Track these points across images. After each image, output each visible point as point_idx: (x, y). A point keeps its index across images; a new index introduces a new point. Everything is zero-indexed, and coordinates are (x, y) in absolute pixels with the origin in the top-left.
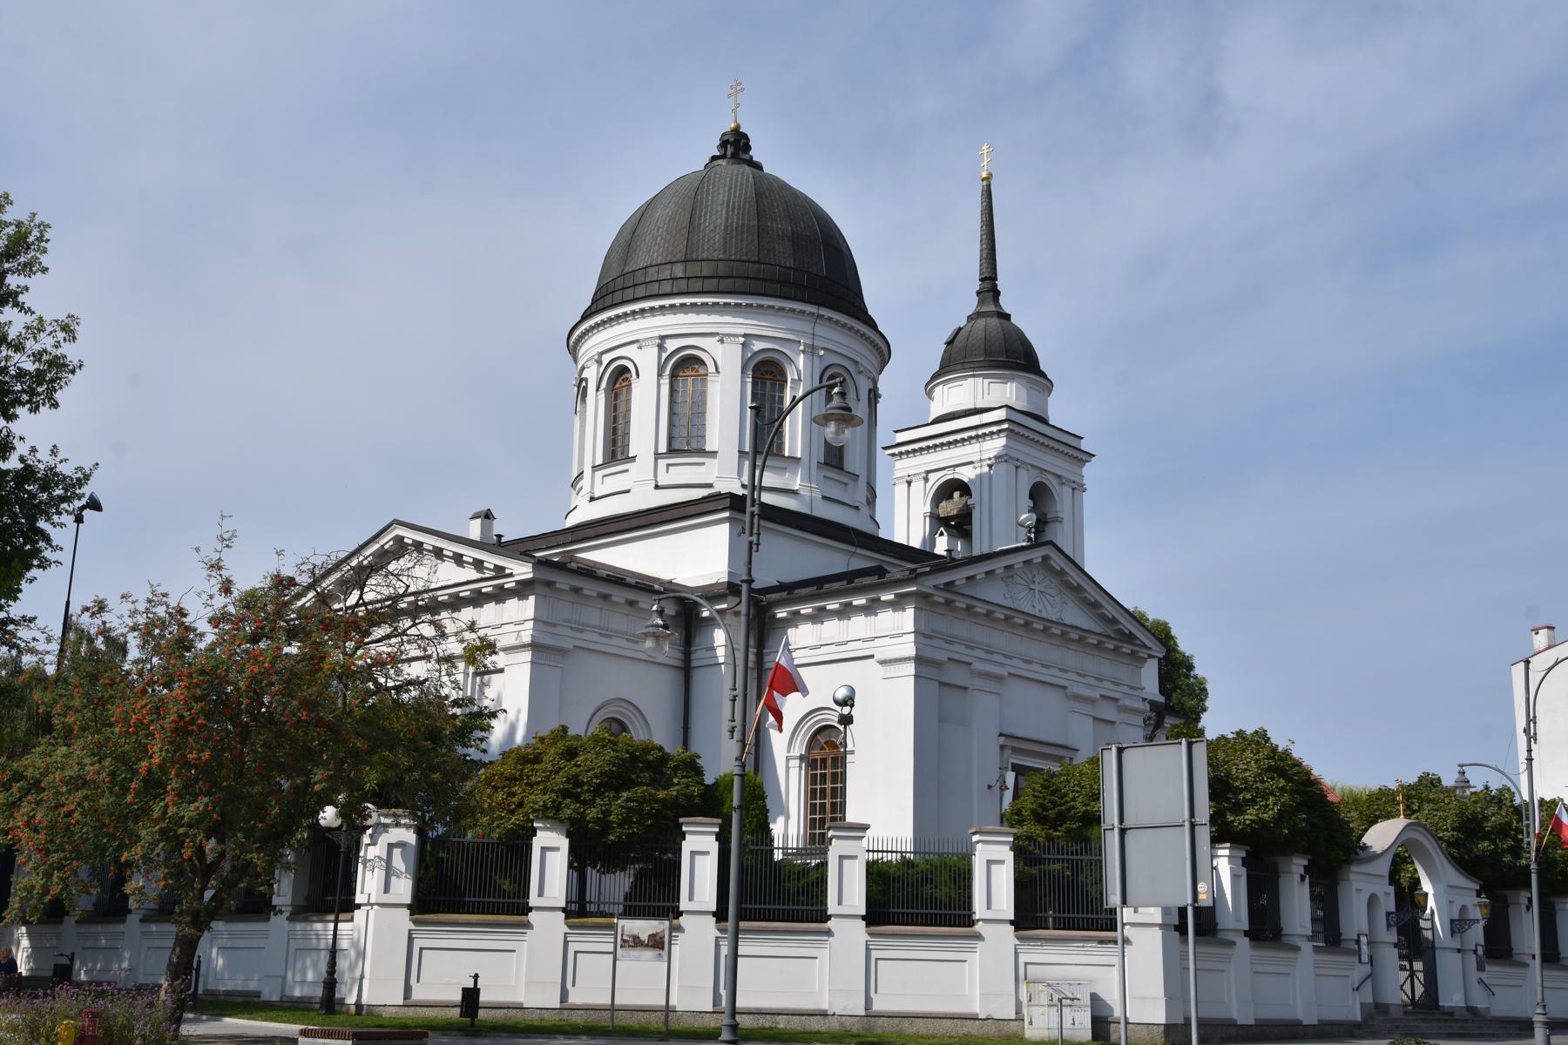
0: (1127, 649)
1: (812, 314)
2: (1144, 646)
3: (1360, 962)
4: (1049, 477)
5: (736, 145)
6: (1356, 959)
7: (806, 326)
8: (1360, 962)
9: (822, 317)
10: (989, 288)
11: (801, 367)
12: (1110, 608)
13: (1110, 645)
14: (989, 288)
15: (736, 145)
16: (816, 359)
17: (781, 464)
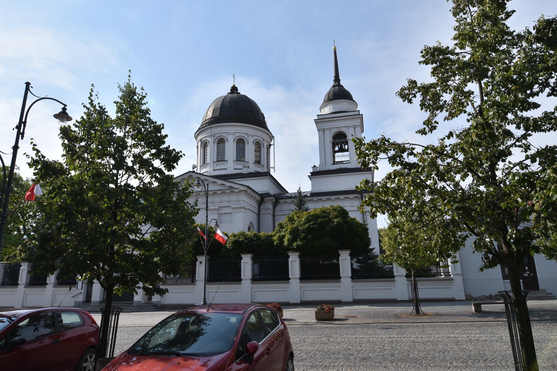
0: (227, 191)
1: (210, 128)
2: (237, 188)
3: (77, 289)
4: (343, 128)
5: (234, 89)
6: (76, 288)
7: (210, 131)
8: (77, 289)
9: (212, 127)
10: (337, 79)
11: (209, 140)
12: (219, 182)
13: (220, 192)
14: (337, 79)
15: (234, 89)
16: (213, 138)
17: (206, 166)
